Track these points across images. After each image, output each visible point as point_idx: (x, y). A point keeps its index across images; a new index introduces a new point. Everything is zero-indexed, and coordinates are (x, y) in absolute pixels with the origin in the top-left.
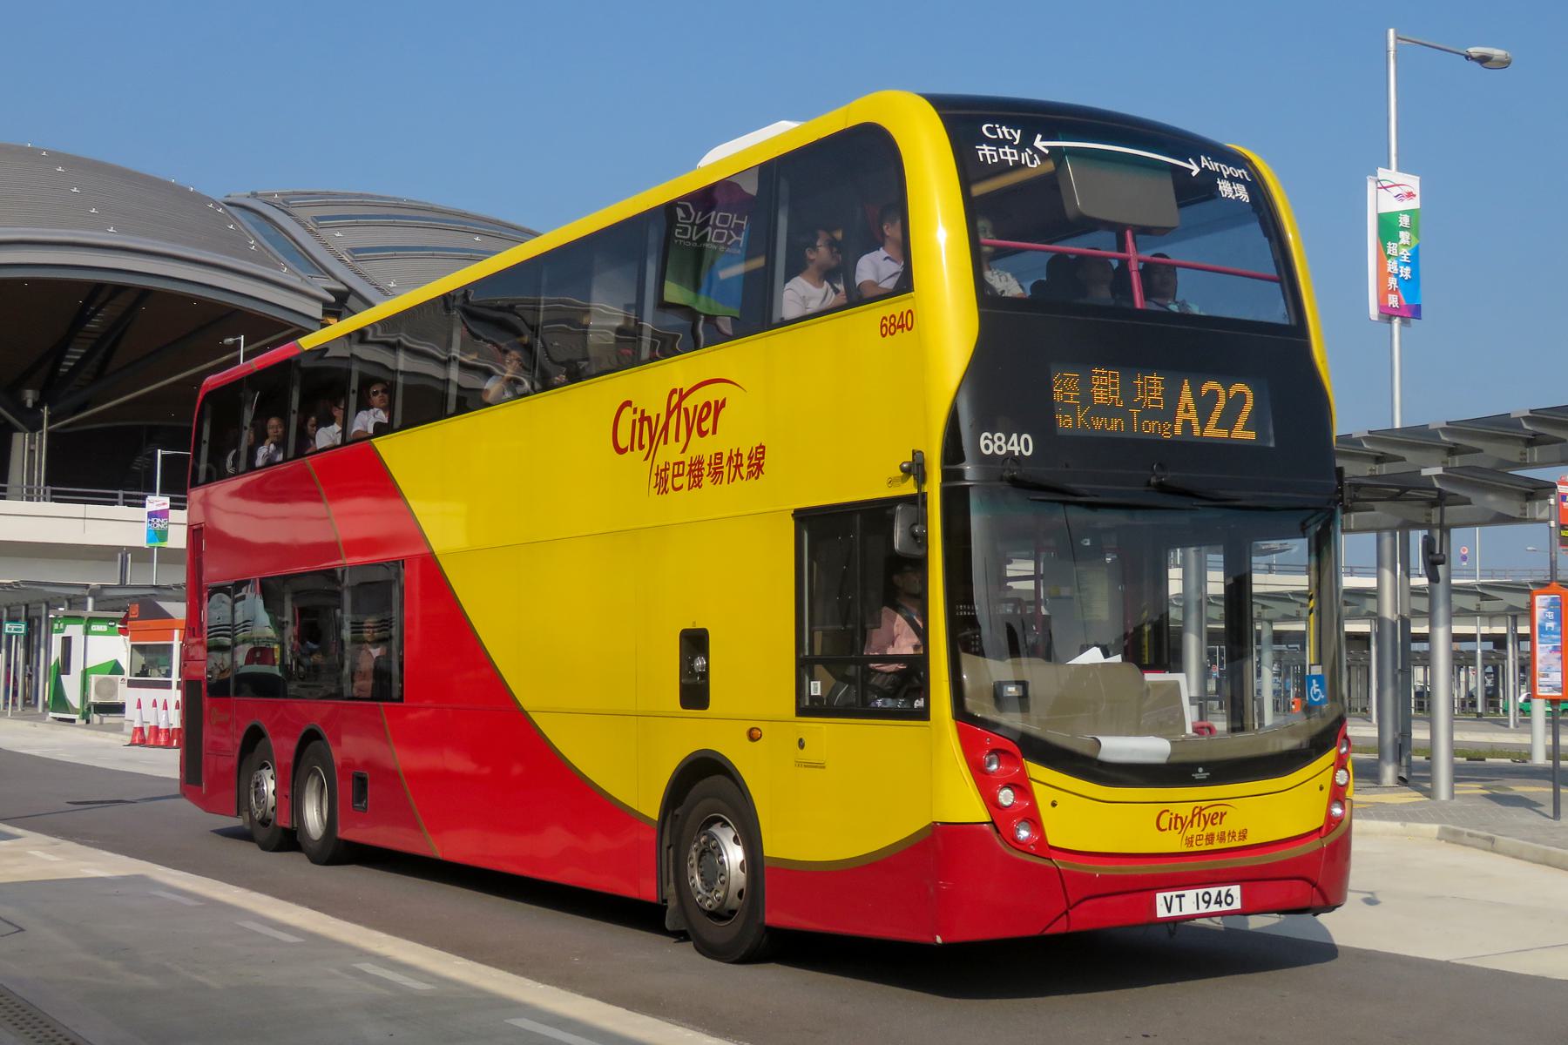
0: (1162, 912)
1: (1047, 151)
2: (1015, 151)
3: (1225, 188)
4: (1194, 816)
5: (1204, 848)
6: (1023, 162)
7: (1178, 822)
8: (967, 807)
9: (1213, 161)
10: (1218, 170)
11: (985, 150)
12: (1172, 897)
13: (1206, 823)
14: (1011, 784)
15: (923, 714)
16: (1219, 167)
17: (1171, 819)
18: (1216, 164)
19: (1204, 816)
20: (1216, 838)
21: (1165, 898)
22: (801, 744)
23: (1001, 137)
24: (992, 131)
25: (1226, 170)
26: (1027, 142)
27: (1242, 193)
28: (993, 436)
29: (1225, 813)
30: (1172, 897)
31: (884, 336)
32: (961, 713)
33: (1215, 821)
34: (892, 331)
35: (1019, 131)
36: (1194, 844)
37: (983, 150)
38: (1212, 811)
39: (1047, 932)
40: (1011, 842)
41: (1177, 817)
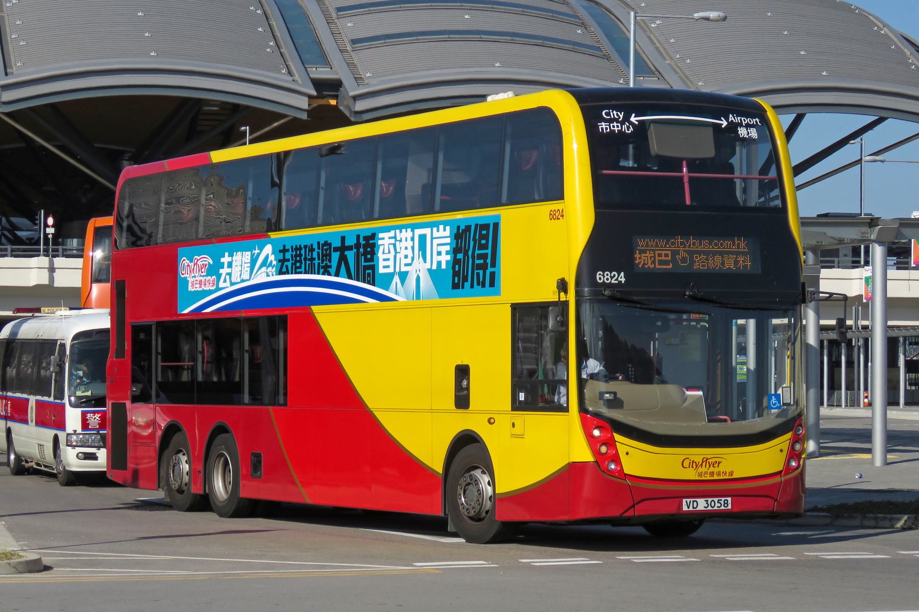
0: (685, 508)
1: (637, 123)
2: (619, 124)
3: (742, 132)
4: (703, 462)
5: (708, 478)
6: (623, 130)
7: (693, 464)
8: (584, 454)
9: (737, 116)
10: (739, 122)
11: (603, 126)
12: (690, 501)
13: (710, 466)
14: (605, 443)
15: (566, 409)
16: (741, 120)
17: (690, 463)
18: (739, 118)
19: (709, 463)
20: (715, 473)
21: (686, 501)
22: (513, 425)
23: (612, 117)
24: (607, 114)
25: (745, 121)
26: (627, 118)
27: (754, 133)
28: (604, 274)
29: (721, 462)
30: (690, 501)
31: (551, 219)
32: (583, 409)
33: (715, 466)
34: (555, 218)
35: (623, 113)
36: (703, 476)
37: (602, 125)
38: (714, 460)
39: (624, 515)
40: (608, 473)
41: (693, 462)
